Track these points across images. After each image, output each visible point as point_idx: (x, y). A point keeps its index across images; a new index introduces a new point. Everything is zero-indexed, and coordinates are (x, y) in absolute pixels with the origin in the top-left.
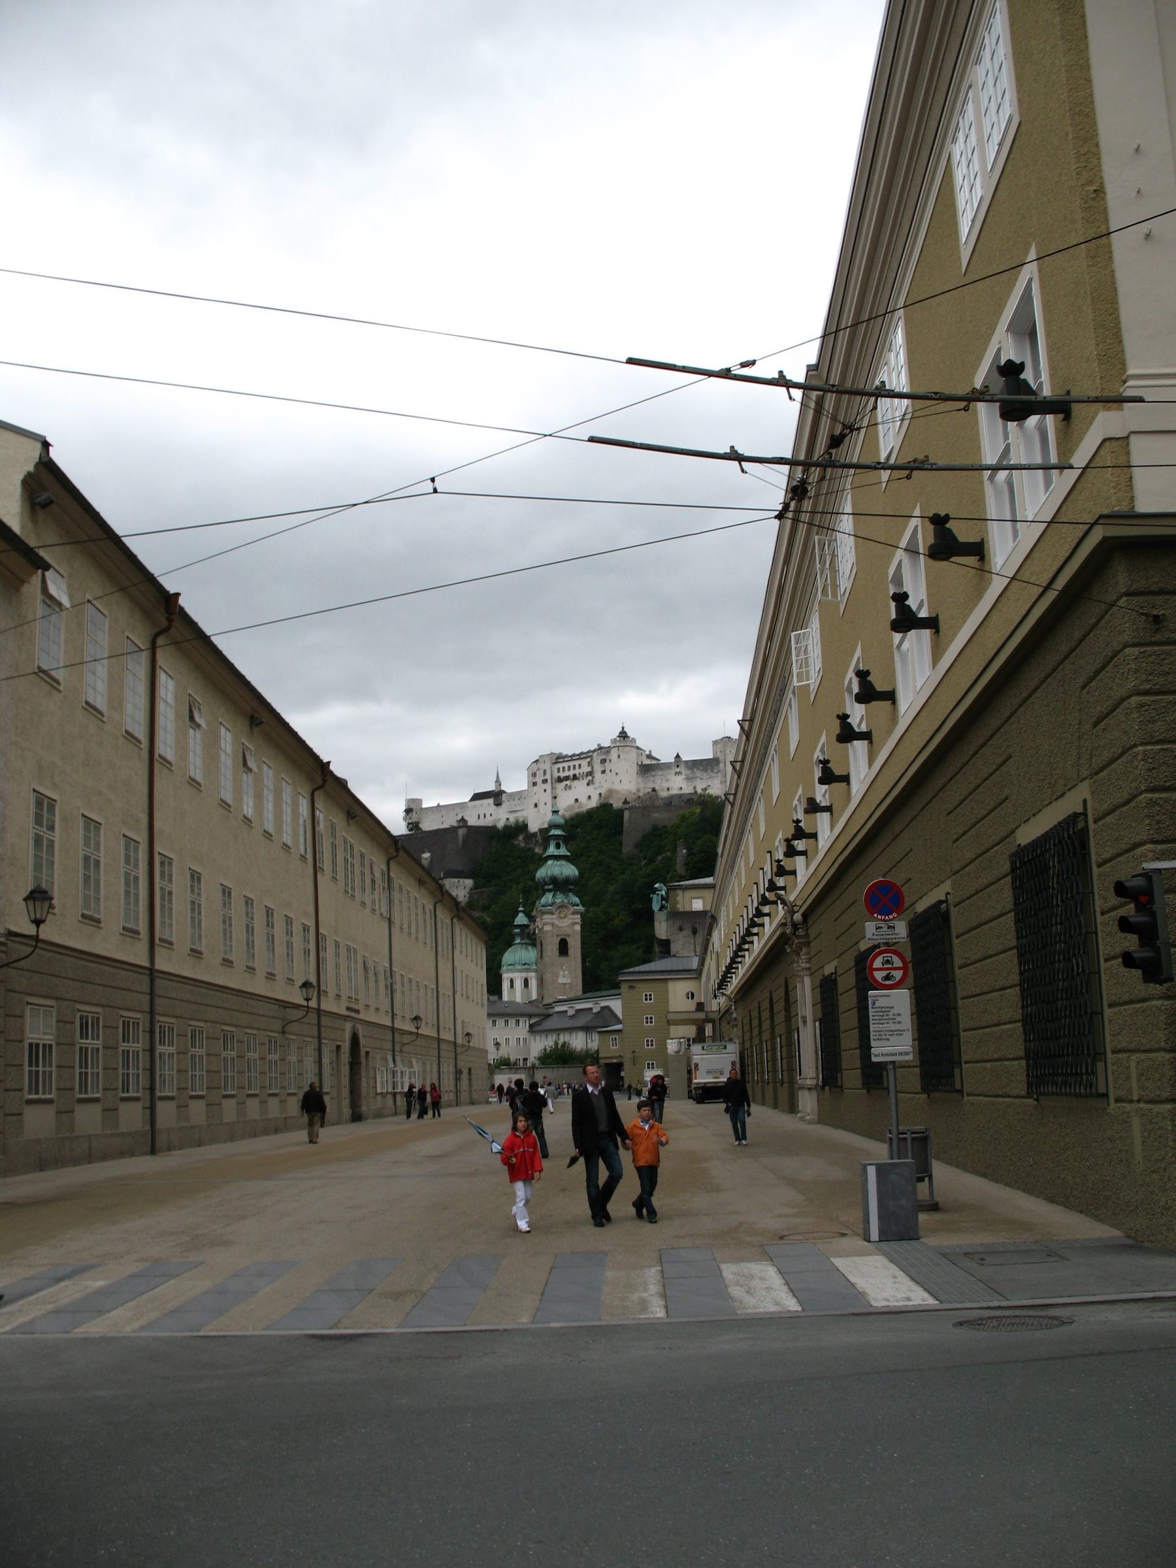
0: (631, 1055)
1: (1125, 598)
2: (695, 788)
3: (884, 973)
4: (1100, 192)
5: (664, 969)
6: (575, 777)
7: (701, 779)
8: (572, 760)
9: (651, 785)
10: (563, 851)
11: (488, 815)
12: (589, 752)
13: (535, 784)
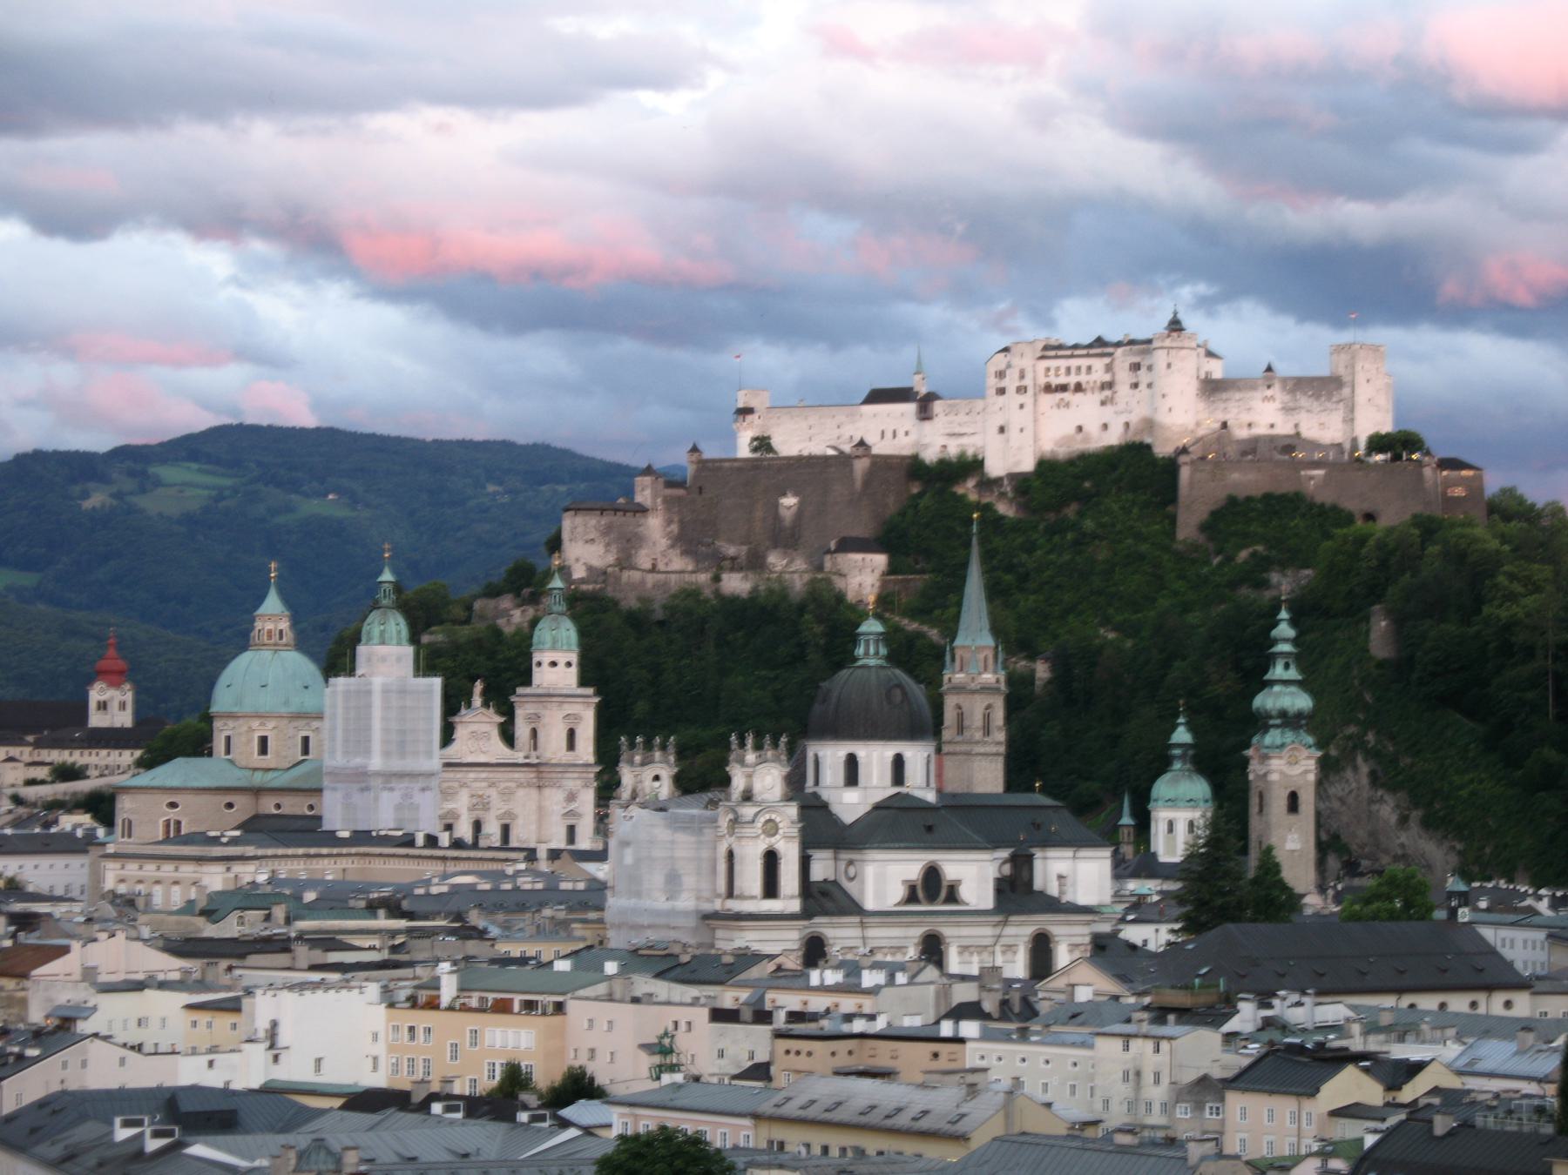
2: (1296, 426)
6: (1079, 388)
7: (1308, 411)
8: (1072, 356)
9: (1221, 417)
10: (1293, 674)
11: (901, 434)
13: (1001, 391)
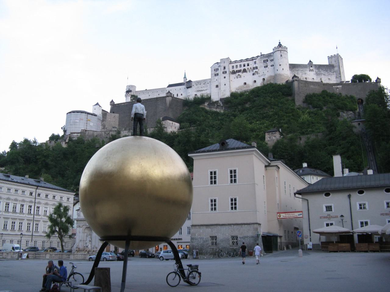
2: (321, 79)
6: (245, 71)
7: (324, 75)
11: (179, 95)
13: (217, 75)
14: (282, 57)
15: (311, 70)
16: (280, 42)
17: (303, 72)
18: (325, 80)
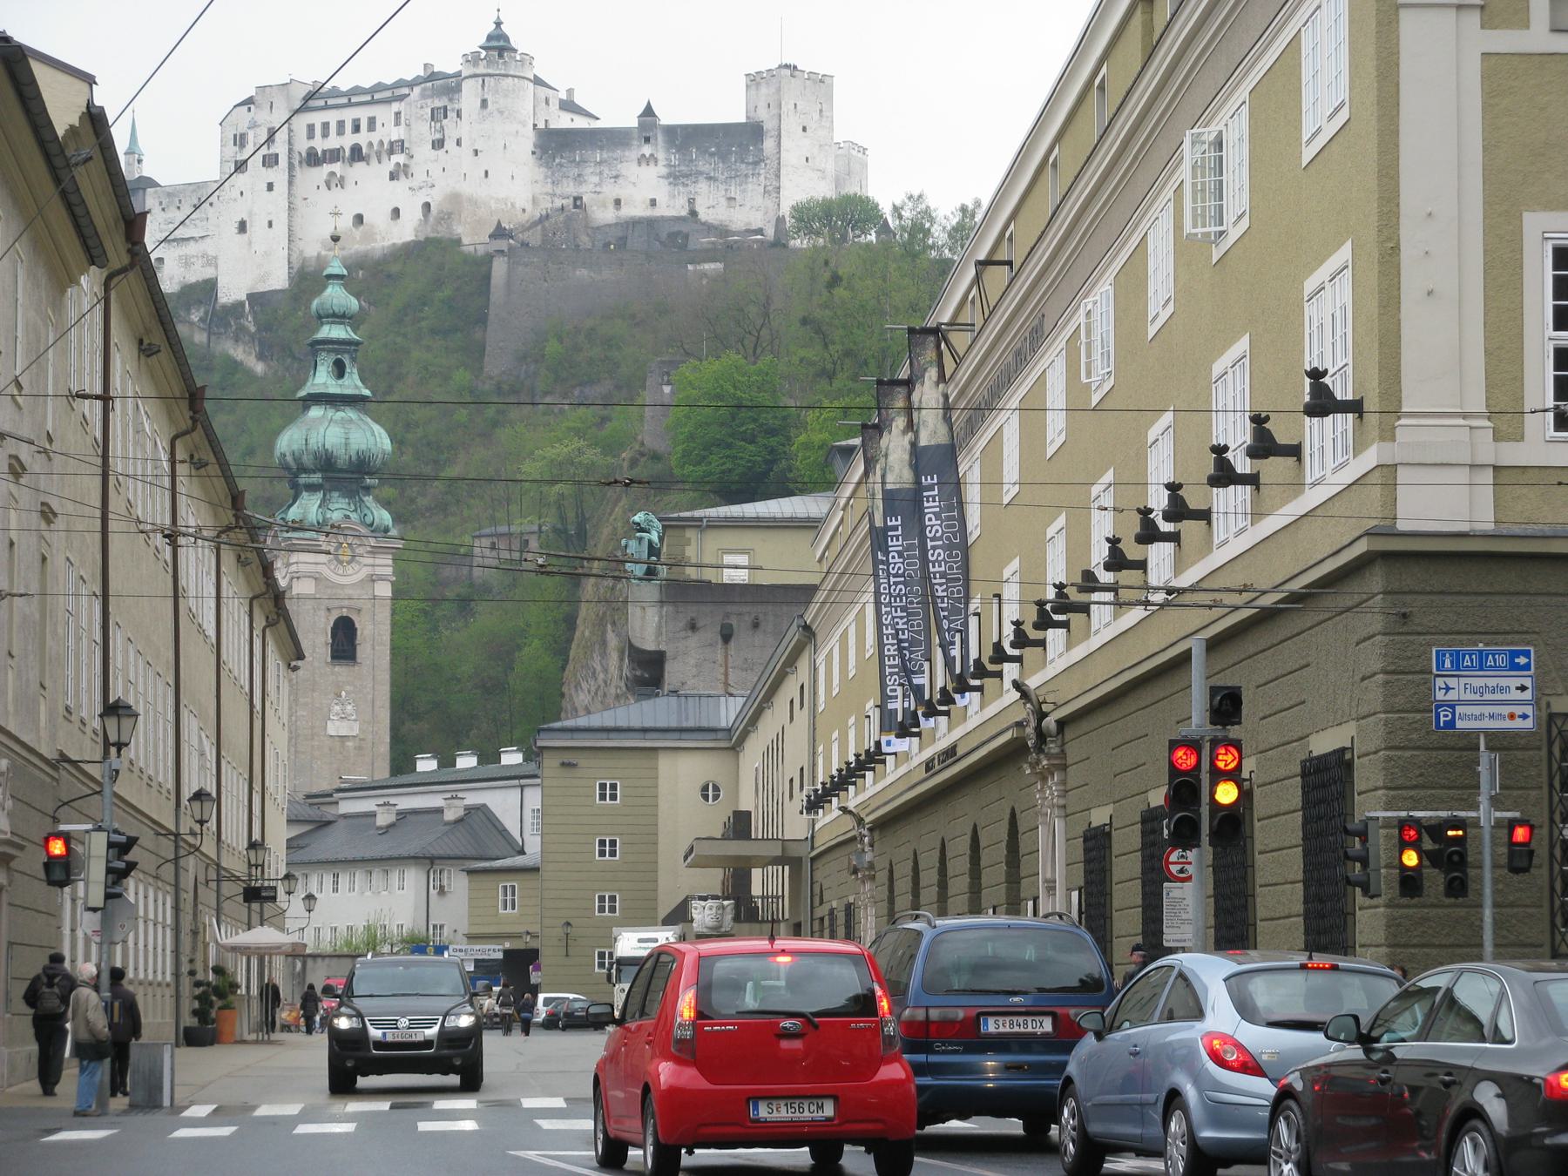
0: (560, 932)
1: (1381, 596)
2: (691, 201)
3: (1179, 867)
4: (1396, 249)
5: (649, 724)
6: (357, 154)
7: (710, 178)
8: (350, 105)
9: (570, 188)
12: (400, 84)
13: (240, 166)
14: (485, 112)
15: (643, 155)
16: (502, 19)
17: (606, 171)
18: (713, 204)
